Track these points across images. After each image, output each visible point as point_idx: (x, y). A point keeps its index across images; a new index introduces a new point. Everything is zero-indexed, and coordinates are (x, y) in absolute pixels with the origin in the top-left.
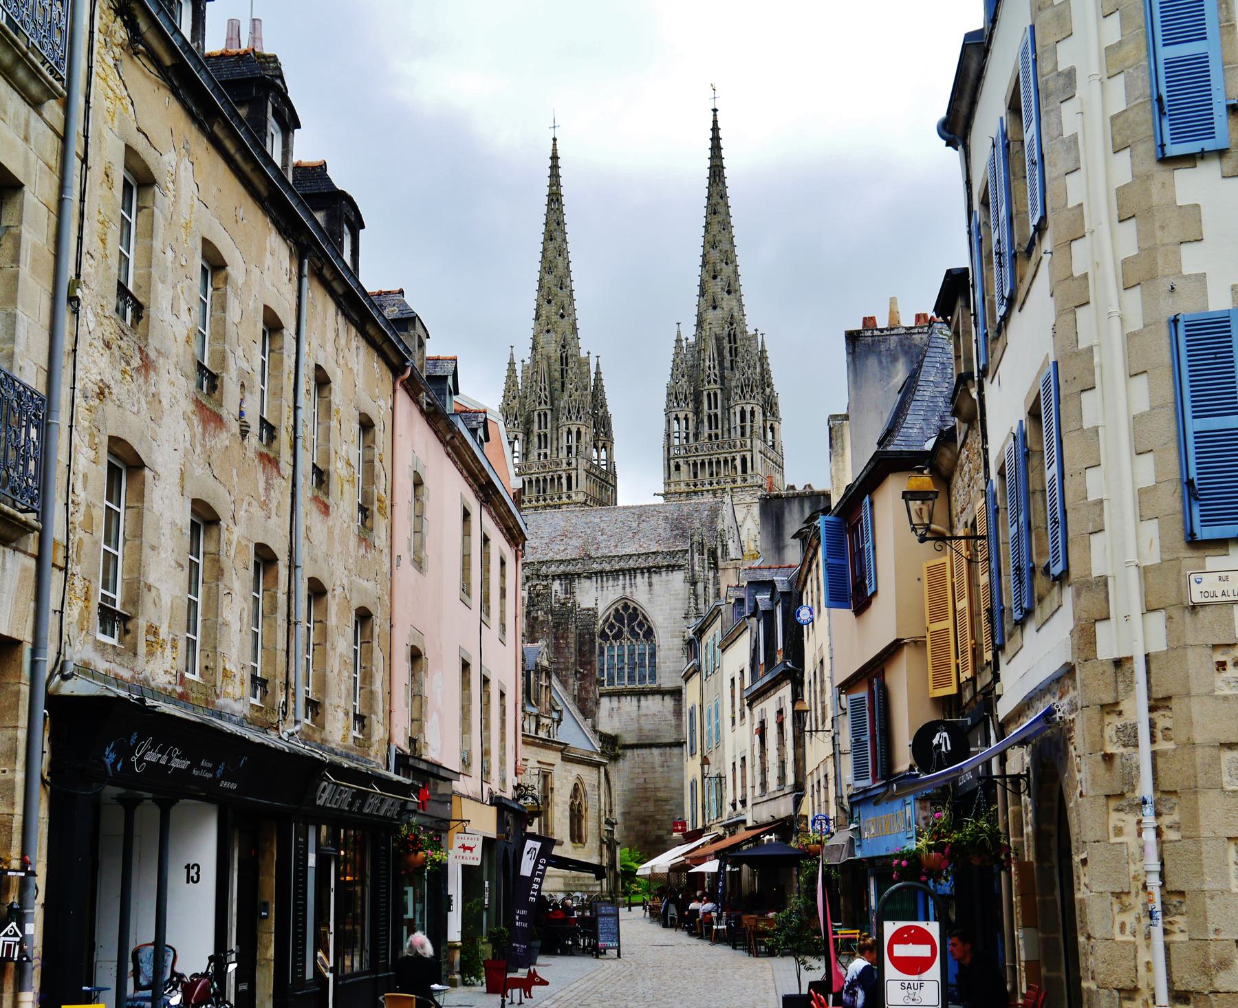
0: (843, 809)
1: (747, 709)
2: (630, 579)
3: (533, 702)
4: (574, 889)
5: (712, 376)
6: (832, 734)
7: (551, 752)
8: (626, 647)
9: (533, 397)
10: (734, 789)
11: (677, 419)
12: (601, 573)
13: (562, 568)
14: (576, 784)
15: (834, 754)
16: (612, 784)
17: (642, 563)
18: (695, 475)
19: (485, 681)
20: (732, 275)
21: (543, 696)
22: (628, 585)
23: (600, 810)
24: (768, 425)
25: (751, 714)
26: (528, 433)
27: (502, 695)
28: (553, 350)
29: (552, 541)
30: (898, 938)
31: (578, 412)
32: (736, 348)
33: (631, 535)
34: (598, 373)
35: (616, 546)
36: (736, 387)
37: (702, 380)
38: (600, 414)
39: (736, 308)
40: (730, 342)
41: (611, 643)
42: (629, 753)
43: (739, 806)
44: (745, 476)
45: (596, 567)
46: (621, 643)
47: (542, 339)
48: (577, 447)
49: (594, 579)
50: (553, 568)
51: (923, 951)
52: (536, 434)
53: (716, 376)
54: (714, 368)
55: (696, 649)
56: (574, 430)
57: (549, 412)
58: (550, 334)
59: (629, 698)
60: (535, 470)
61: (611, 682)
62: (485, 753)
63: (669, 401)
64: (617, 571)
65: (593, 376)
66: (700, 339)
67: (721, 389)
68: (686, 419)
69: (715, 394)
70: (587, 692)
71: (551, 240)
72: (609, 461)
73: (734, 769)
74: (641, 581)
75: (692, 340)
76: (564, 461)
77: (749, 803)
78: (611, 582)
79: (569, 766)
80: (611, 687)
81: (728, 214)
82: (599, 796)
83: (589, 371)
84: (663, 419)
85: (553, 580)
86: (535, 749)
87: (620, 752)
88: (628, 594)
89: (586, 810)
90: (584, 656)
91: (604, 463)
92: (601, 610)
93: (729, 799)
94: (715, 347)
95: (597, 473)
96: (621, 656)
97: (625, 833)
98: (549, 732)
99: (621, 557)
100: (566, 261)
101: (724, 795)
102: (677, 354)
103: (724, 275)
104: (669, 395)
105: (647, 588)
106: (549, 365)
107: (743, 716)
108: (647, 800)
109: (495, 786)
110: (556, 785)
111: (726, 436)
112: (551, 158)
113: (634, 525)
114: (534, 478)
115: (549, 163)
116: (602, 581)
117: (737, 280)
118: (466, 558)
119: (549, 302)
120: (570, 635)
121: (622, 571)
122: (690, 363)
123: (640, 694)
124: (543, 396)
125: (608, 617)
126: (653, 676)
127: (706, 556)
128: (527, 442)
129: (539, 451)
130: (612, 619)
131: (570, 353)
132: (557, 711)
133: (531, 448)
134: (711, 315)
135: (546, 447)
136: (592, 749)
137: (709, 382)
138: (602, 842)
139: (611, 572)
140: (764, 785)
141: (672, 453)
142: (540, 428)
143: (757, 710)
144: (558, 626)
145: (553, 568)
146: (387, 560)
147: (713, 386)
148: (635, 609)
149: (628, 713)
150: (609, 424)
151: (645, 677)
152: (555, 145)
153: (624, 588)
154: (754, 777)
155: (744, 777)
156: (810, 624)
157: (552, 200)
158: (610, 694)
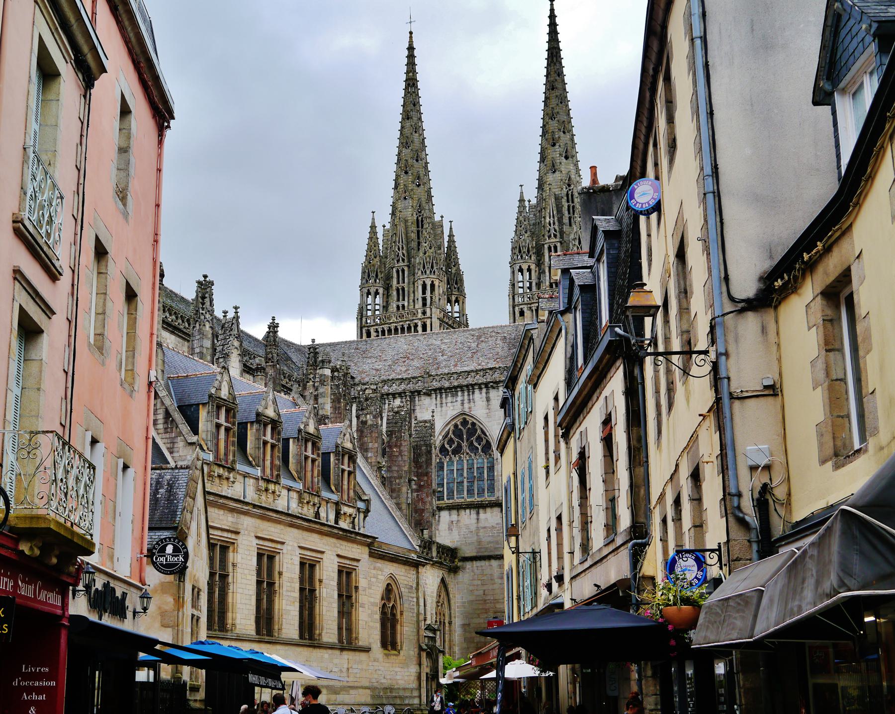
0: (743, 523)
1: (561, 440)
2: (469, 395)
3: (333, 488)
4: (385, 702)
5: (553, 231)
6: (713, 356)
7: (355, 546)
8: (465, 461)
9: (393, 256)
10: (550, 566)
11: (521, 270)
12: (440, 390)
13: (403, 386)
14: (388, 585)
15: (717, 408)
16: (451, 596)
17: (479, 379)
20: (569, 143)
21: (345, 482)
22: (466, 401)
23: (418, 614)
26: (387, 288)
28: (409, 214)
29: (395, 362)
31: (432, 267)
32: (573, 207)
34: (451, 236)
36: (574, 239)
37: (544, 236)
38: (453, 271)
39: (573, 172)
40: (568, 201)
42: (468, 565)
43: (555, 585)
45: (436, 384)
46: (460, 457)
47: (400, 205)
48: (431, 298)
49: (434, 396)
50: (395, 387)
52: (394, 288)
53: (555, 230)
54: (554, 224)
56: (428, 283)
57: (406, 269)
58: (407, 201)
59: (468, 511)
60: (394, 319)
61: (451, 495)
63: (514, 254)
64: (455, 387)
65: (446, 239)
66: (541, 199)
67: (561, 242)
68: (529, 270)
70: (424, 503)
71: (408, 119)
72: (462, 313)
75: (534, 201)
76: (420, 311)
77: (567, 578)
78: (450, 399)
79: (380, 564)
80: (451, 501)
81: (565, 89)
82: (418, 599)
83: (442, 232)
85: (394, 398)
86: (333, 540)
87: (460, 564)
88: (467, 410)
89: (402, 614)
90: (421, 467)
92: (439, 426)
93: (544, 577)
94: (554, 205)
95: (450, 323)
97: (465, 645)
98: (353, 522)
99: (459, 374)
100: (421, 137)
101: (539, 577)
102: (520, 212)
103: (562, 142)
104: (513, 249)
105: (485, 403)
106: (406, 228)
108: (486, 611)
110: (362, 583)
112: (408, 49)
113: (474, 345)
114: (393, 326)
115: (406, 53)
116: (441, 397)
117: (573, 147)
119: (406, 173)
120: (404, 443)
121: (461, 387)
122: (532, 222)
123: (479, 507)
124: (401, 254)
126: (491, 489)
128: (387, 295)
130: (451, 435)
131: (425, 215)
132: (364, 501)
133: (390, 301)
134: (550, 178)
135: (404, 300)
136: (409, 547)
137: (550, 237)
138: (421, 649)
139: (450, 388)
140: (585, 547)
142: (398, 283)
144: (391, 435)
145: (395, 387)
147: (553, 240)
148: (473, 424)
150: (462, 280)
151: (484, 490)
152: (411, 37)
153: (463, 404)
154: (572, 538)
155: (560, 545)
156: (654, 216)
157: (409, 84)
158: (450, 508)
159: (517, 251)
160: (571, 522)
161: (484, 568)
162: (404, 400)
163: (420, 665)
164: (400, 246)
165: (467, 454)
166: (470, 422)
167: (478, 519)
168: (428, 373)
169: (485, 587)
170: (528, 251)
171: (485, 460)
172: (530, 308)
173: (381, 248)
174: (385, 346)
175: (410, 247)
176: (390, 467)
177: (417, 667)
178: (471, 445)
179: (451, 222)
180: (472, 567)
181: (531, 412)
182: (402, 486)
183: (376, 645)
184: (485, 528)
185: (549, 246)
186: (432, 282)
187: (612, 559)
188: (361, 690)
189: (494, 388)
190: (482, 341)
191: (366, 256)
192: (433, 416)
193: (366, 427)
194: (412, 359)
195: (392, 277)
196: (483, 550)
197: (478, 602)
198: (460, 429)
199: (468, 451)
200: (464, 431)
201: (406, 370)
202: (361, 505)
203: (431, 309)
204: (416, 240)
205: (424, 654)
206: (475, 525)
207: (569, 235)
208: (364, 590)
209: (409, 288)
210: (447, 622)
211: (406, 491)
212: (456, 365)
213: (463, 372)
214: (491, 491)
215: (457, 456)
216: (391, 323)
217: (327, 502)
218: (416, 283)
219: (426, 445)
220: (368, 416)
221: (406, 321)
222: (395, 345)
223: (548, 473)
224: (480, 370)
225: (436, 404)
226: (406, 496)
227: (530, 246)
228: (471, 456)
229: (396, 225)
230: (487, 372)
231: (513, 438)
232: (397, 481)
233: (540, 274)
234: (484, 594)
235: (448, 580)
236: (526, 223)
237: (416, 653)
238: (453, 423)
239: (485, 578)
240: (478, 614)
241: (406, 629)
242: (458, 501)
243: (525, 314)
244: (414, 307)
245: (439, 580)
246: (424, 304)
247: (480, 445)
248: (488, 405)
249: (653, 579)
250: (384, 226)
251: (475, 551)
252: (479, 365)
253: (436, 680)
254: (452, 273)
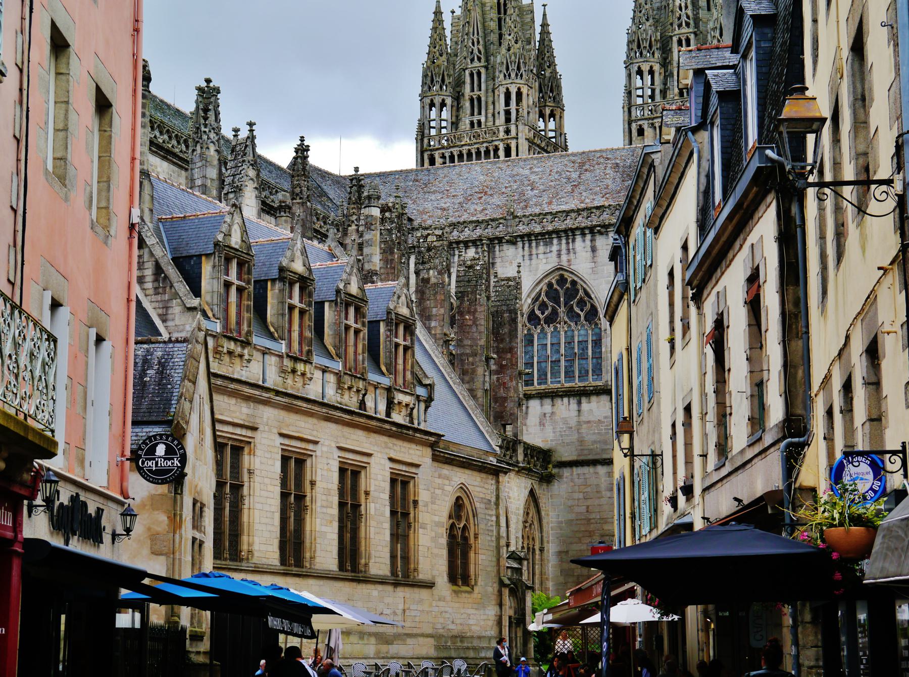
1: (691, 304)
2: (568, 243)
3: (384, 368)
4: (453, 654)
5: (684, 18)
6: (898, 187)
7: (413, 446)
8: (562, 333)
9: (465, 54)
10: (675, 473)
11: (640, 72)
12: (528, 237)
13: (478, 232)
14: (458, 498)
16: (543, 513)
17: (582, 222)
21: (400, 361)
22: (564, 252)
23: (498, 538)
26: (458, 98)
29: (467, 200)
31: (519, 68)
33: (569, 188)
34: (544, 25)
35: (550, 203)
36: (714, 29)
37: (672, 24)
38: (548, 74)
41: (543, 329)
42: (566, 472)
43: (681, 499)
45: (523, 229)
46: (555, 328)
48: (517, 111)
49: (520, 244)
52: (467, 97)
53: (688, 17)
54: (686, 7)
56: (513, 90)
57: (483, 71)
59: (566, 400)
60: (466, 140)
61: (543, 379)
63: (630, 49)
64: (550, 233)
65: (538, 29)
67: (695, 34)
68: (651, 72)
70: (507, 389)
72: (559, 131)
74: (581, 245)
76: (502, 129)
77: (697, 490)
78: (542, 249)
79: (447, 470)
80: (543, 387)
82: (498, 517)
83: (533, 20)
84: (623, 73)
85: (467, 247)
87: (555, 471)
88: (565, 263)
89: (476, 537)
90: (502, 340)
92: (527, 285)
93: (667, 487)
95: (543, 145)
96: (556, 345)
97: (562, 579)
98: (411, 415)
99: (554, 215)
101: (660, 488)
104: (630, 42)
105: (589, 254)
106: (483, 14)
108: (590, 534)
110: (423, 496)
113: (574, 175)
114: (465, 150)
116: (530, 246)
120: (479, 309)
121: (557, 232)
123: (581, 394)
124: (476, 51)
125: (539, 294)
126: (598, 370)
128: (457, 108)
129: (472, 118)
130: (543, 297)
132: (425, 386)
133: (462, 115)
135: (480, 113)
136: (485, 447)
137: (680, 26)
138: (502, 584)
139: (542, 234)
140: (723, 448)
141: (633, 114)
142: (472, 90)
144: (463, 297)
145: (467, 232)
147: (685, 30)
148: (574, 283)
149: (565, 421)
150: (559, 87)
151: (587, 372)
153: (559, 255)
154: (705, 435)
155: (688, 445)
158: (542, 396)
159: (635, 46)
160: (704, 415)
161: (587, 476)
162: (480, 250)
163: (501, 605)
164: (475, 40)
165: (565, 323)
166: (569, 280)
167: (579, 411)
168: (512, 213)
169: (589, 502)
170: (651, 46)
171: (590, 332)
172: (652, 124)
173: (448, 42)
174: (454, 177)
175: (489, 40)
176: (461, 340)
177: (497, 608)
178: (571, 310)
179: (544, 6)
180: (572, 475)
181: (651, 266)
182: (477, 366)
183: (442, 579)
184: (589, 422)
185: (680, 38)
186: (519, 89)
187: (758, 464)
188: (421, 639)
189: (600, 233)
190: (586, 170)
191: (428, 54)
192: (519, 272)
193: (429, 286)
194: (491, 195)
195: (464, 83)
196: (586, 452)
197: (579, 522)
198: (556, 290)
199: (566, 319)
200: (562, 292)
201: (483, 210)
202: (421, 391)
203: (517, 126)
204: (497, 31)
205: (506, 592)
206: (576, 419)
207: (706, 23)
208: (426, 505)
209: (487, 97)
210: (537, 547)
211: (482, 373)
212: (550, 203)
213: (560, 212)
214: (597, 372)
215: (551, 325)
216: (462, 145)
217: (376, 388)
218: (496, 91)
219: (510, 311)
220: (431, 272)
221: (483, 142)
222: (467, 175)
223: (673, 348)
224: (583, 210)
225: (523, 256)
226: (482, 380)
227: (653, 39)
228: (570, 326)
229: (469, 11)
230: (592, 213)
231: (626, 301)
232: (471, 359)
233: (666, 77)
234: (587, 511)
235: (538, 492)
236: (647, 7)
237: (496, 589)
238: (546, 281)
239: (589, 489)
240: (580, 539)
241: (481, 557)
242: (552, 386)
243: (646, 133)
244: (494, 124)
245: (527, 492)
246: (508, 120)
247: (582, 310)
248: (594, 257)
249: (813, 490)
250: (453, 12)
251: (575, 453)
252: (582, 202)
253: (522, 626)
254: (545, 77)
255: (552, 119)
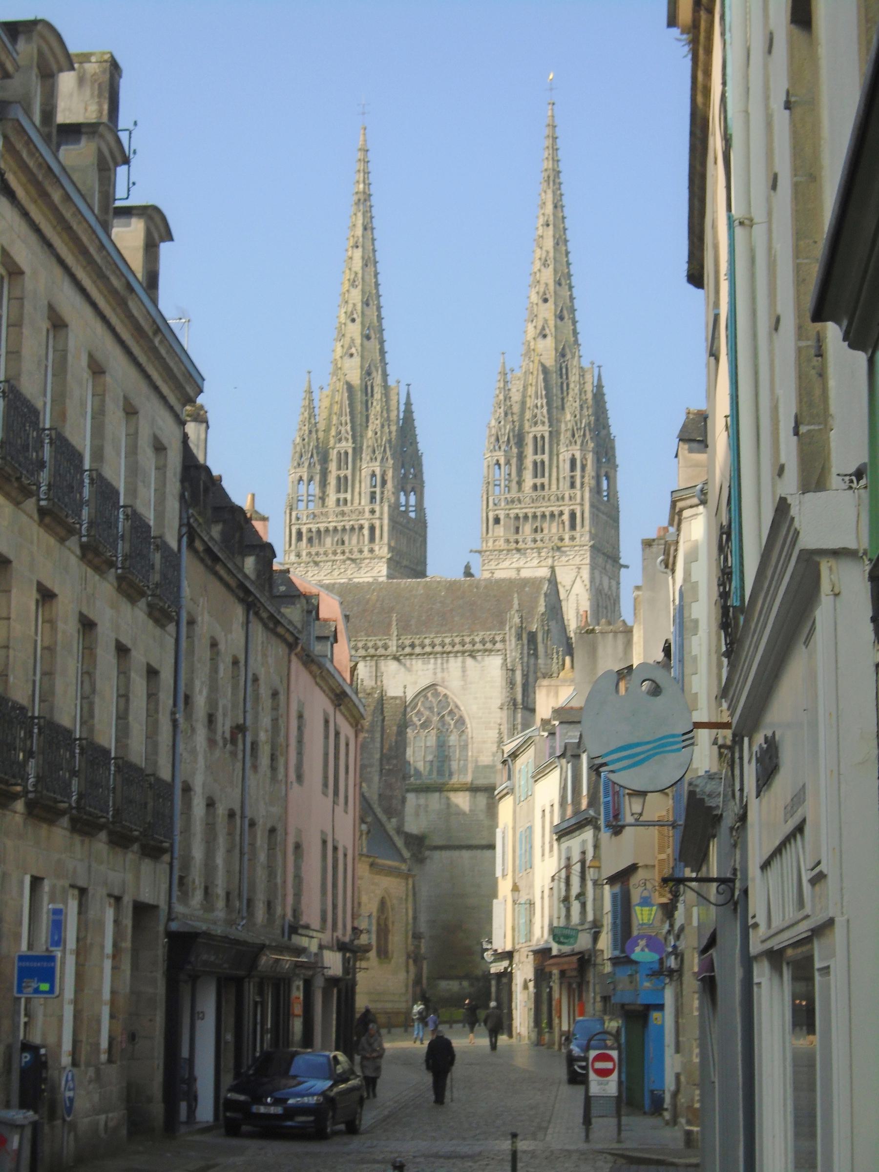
1: (555, 844)
2: (442, 664)
18: (517, 530)
19: (335, 849)
24: (603, 472)
25: (559, 850)
27: (345, 855)
30: (598, 1058)
42: (437, 854)
44: (573, 533)
51: (609, 1065)
55: (509, 769)
62: (335, 906)
69: (543, 437)
72: (420, 508)
73: (542, 898)
79: (378, 878)
82: (407, 909)
89: (393, 923)
91: (413, 509)
101: (533, 921)
107: (551, 847)
109: (339, 933)
110: (364, 899)
111: (554, 487)
118: (326, 754)
127: (525, 641)
128: (324, 484)
135: (346, 491)
143: (564, 846)
146: (283, 787)
150: (420, 465)
153: (435, 674)
163: (408, 972)
172: (508, 514)
177: (405, 974)
179: (409, 385)
192: (405, 693)
205: (411, 961)
216: (330, 522)
223: (543, 855)
255: (412, 493)
